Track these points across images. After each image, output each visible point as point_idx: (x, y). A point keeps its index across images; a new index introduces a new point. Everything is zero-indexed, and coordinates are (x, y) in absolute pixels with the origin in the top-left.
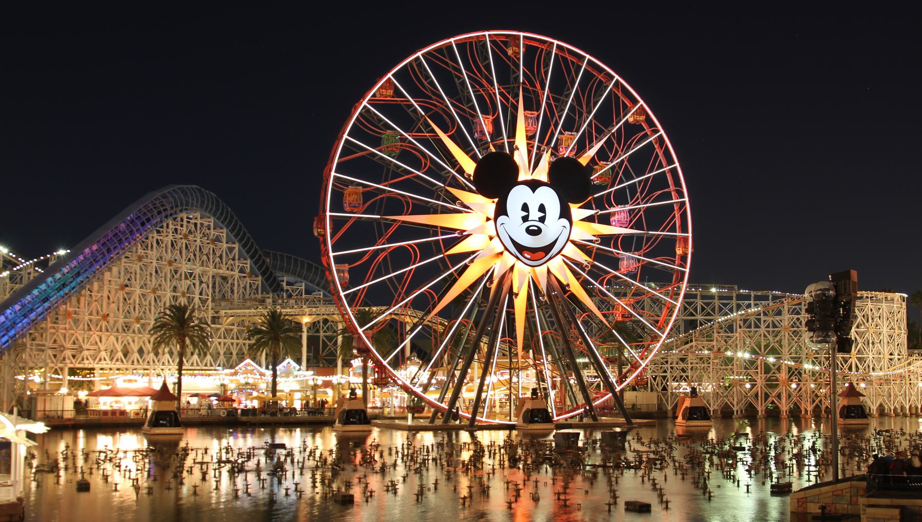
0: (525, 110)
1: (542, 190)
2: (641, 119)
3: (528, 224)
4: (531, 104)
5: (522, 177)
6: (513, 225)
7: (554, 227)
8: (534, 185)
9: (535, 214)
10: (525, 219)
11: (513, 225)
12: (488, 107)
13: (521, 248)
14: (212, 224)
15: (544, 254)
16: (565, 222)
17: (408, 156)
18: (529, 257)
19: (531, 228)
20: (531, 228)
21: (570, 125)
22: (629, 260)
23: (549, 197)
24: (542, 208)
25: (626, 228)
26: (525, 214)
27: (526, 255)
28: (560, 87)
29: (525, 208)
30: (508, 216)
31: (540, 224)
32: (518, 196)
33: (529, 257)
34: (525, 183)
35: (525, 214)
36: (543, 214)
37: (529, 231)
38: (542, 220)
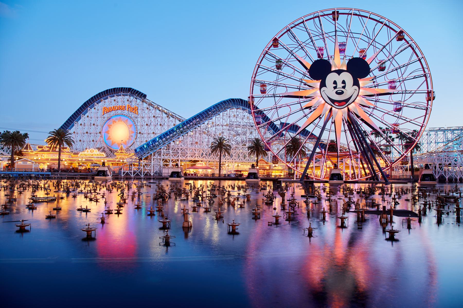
1: (343, 74)
3: (336, 90)
5: (333, 69)
6: (330, 91)
7: (350, 90)
8: (339, 72)
9: (340, 85)
10: (335, 88)
11: (330, 91)
13: (333, 101)
14: (248, 112)
15: (345, 103)
16: (356, 87)
18: (337, 105)
19: (338, 92)
20: (338, 92)
23: (348, 77)
24: (344, 82)
27: (336, 104)
29: (335, 82)
30: (326, 87)
31: (343, 90)
33: (337, 105)
34: (335, 71)
37: (337, 93)
38: (344, 87)
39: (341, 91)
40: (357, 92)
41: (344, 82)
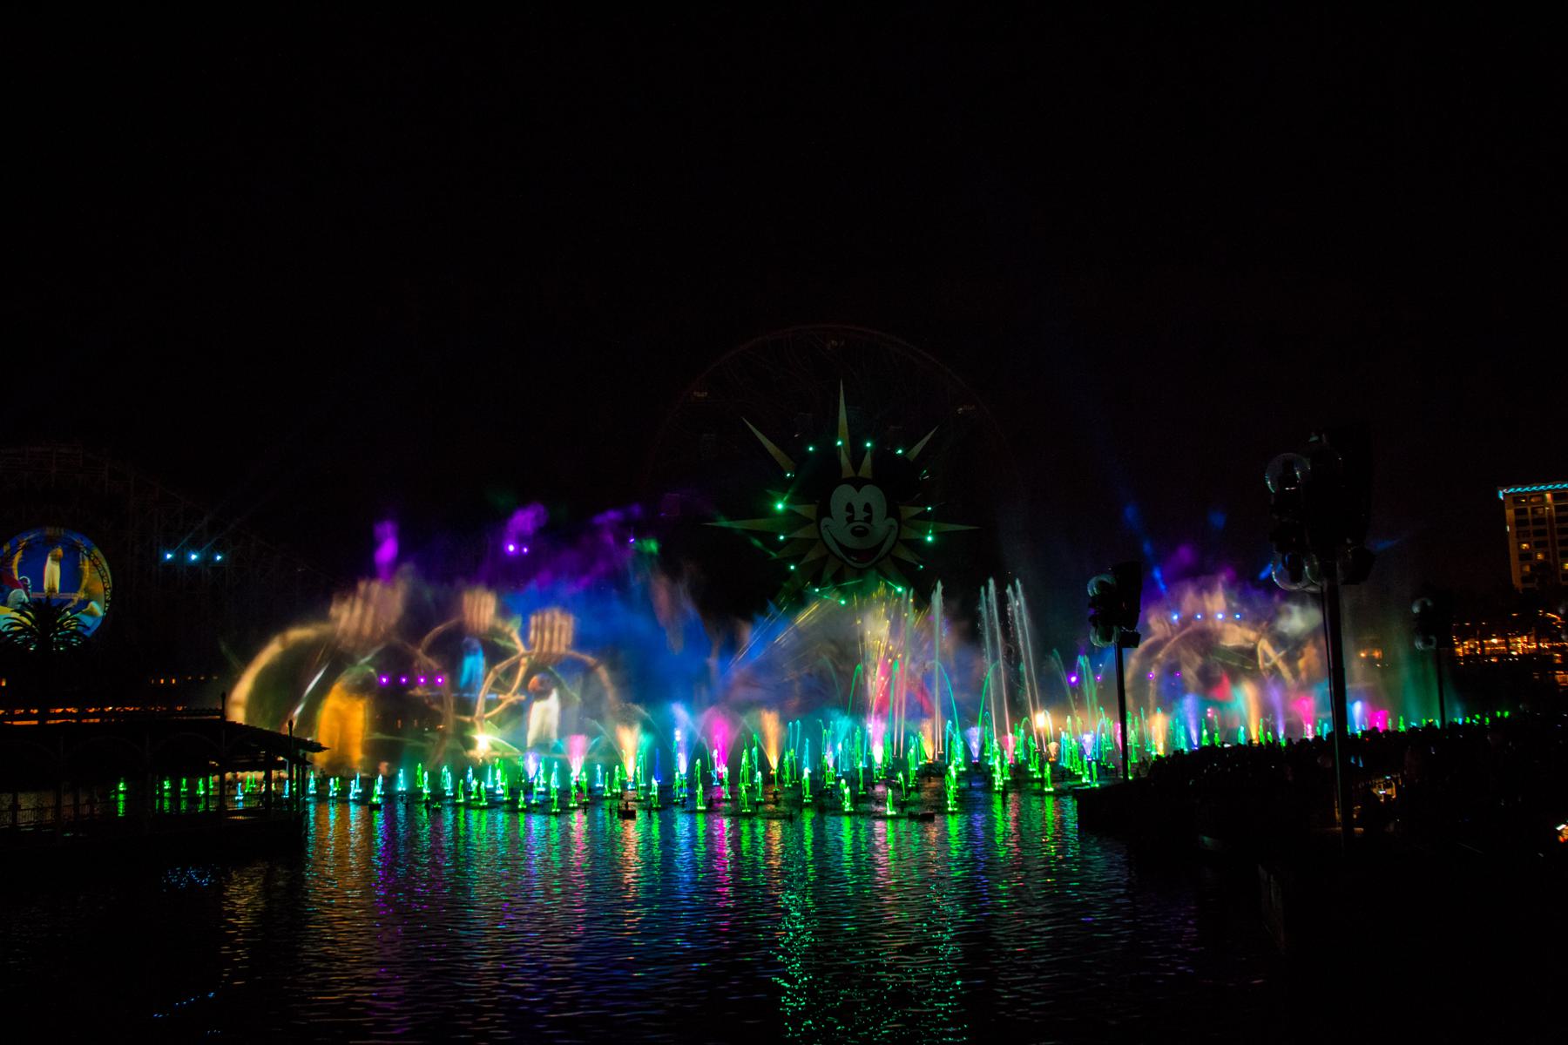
1: (867, 489)
7: (881, 525)
8: (858, 483)
9: (860, 515)
10: (850, 520)
13: (847, 551)
16: (892, 521)
18: (855, 559)
24: (867, 508)
26: (849, 514)
27: (853, 558)
29: (850, 508)
32: (843, 495)
33: (855, 559)
35: (849, 514)
36: (867, 514)
37: (853, 532)
38: (868, 520)
40: (894, 533)
41: (867, 508)
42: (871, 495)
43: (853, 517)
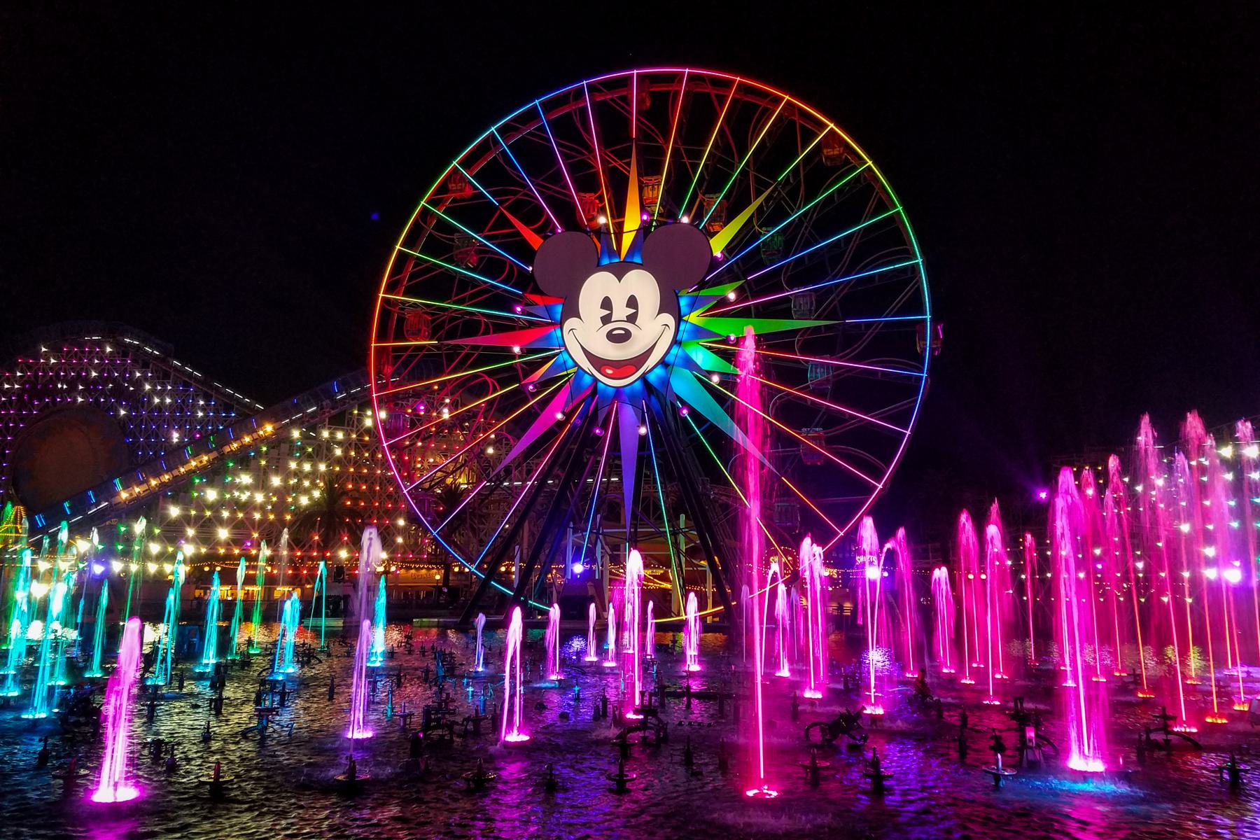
0: (640, 175)
2: (836, 153)
3: (610, 327)
4: (650, 168)
9: (621, 311)
10: (606, 320)
12: (587, 183)
16: (668, 319)
17: (492, 266)
19: (614, 333)
20: (614, 333)
21: (713, 182)
22: (819, 365)
24: (632, 302)
25: (810, 319)
27: (609, 371)
28: (694, 135)
29: (607, 303)
31: (628, 326)
37: (611, 337)
38: (632, 319)
39: (623, 332)
42: (643, 285)
43: (610, 316)
